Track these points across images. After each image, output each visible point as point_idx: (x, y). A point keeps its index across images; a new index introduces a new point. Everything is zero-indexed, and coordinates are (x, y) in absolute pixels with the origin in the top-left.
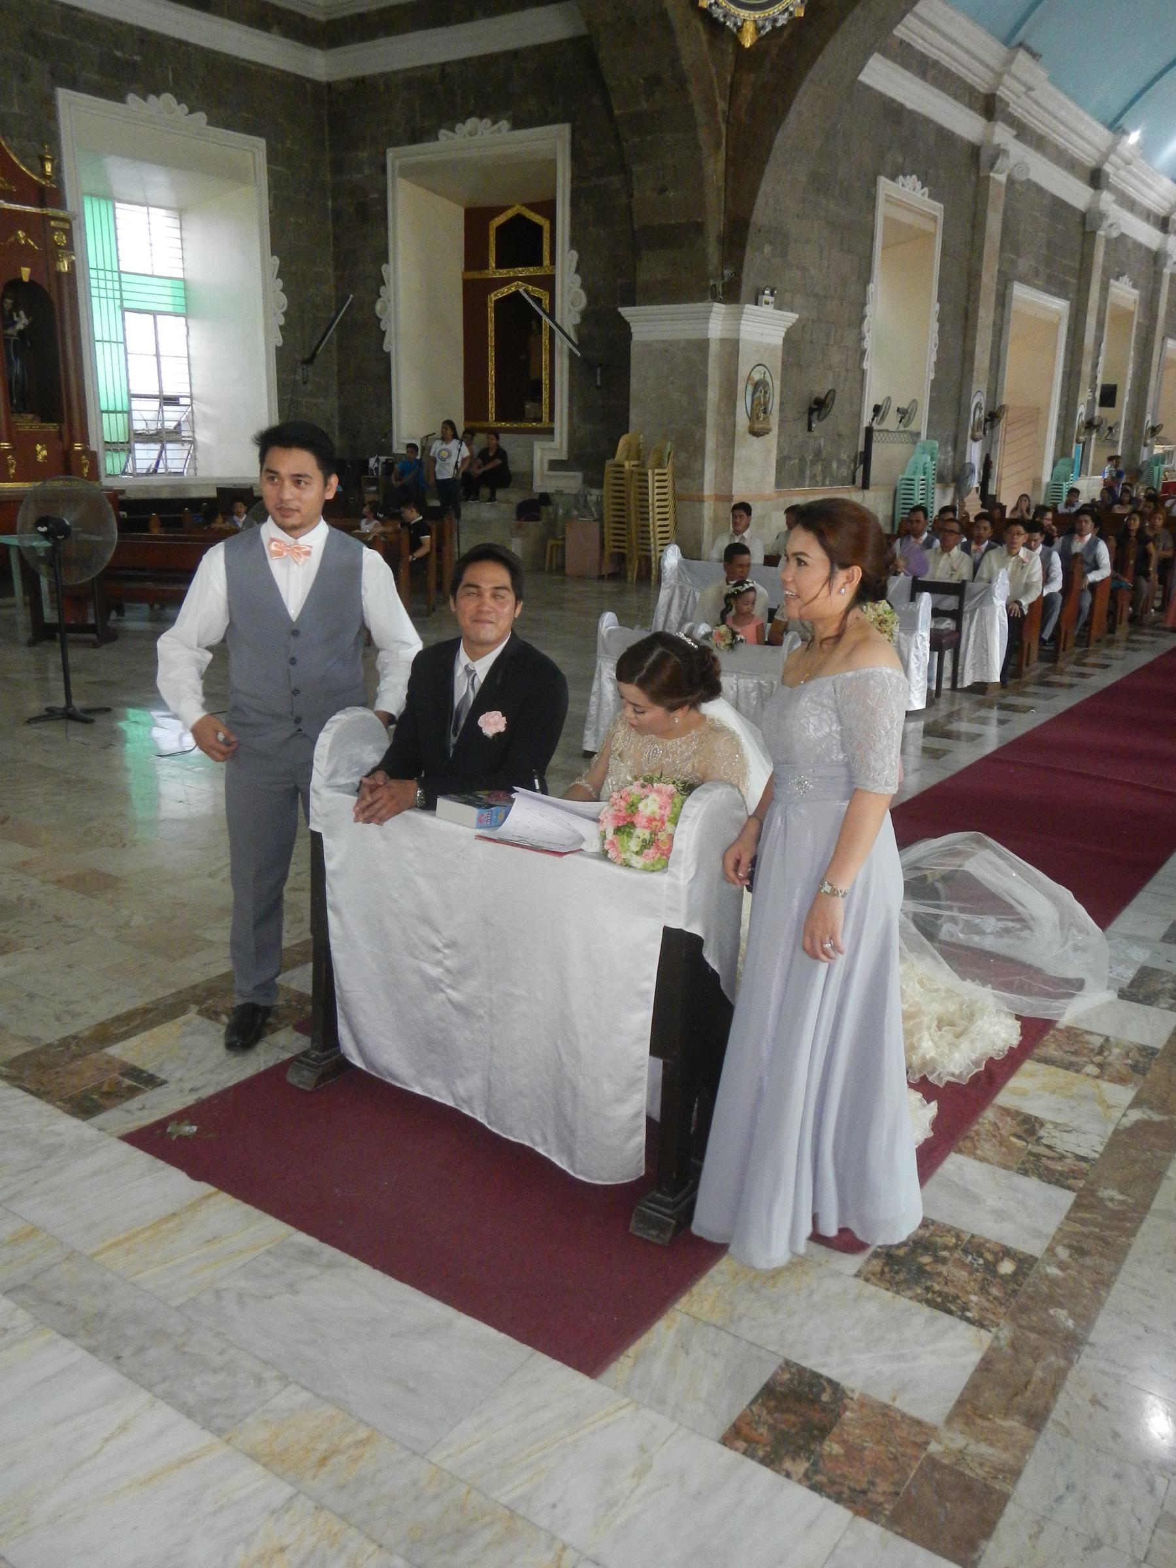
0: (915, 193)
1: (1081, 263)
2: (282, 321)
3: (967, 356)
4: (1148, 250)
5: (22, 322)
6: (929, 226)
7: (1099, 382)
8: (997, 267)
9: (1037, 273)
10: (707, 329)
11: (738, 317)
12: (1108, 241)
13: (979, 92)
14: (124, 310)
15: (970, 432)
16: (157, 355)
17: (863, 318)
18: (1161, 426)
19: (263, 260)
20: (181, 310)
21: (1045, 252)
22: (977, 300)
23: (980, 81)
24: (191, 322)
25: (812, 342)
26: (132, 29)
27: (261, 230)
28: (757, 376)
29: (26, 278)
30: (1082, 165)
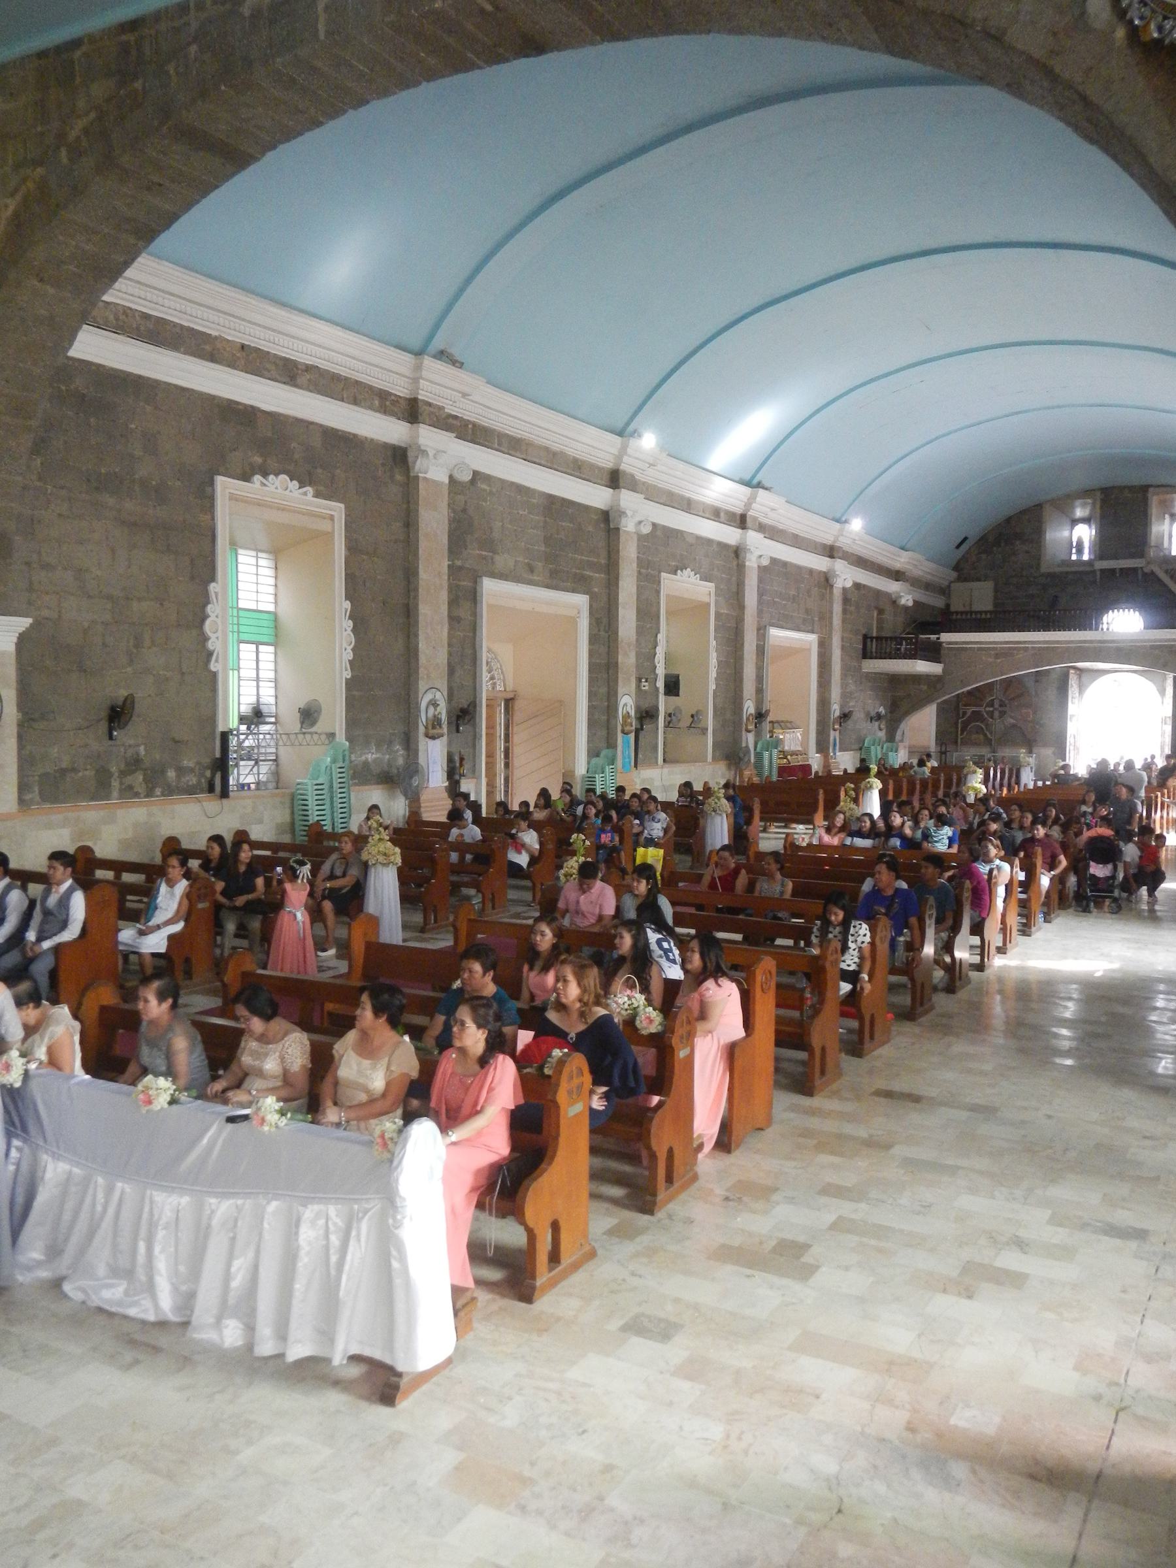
0: (287, 492)
1: (609, 557)
3: (411, 654)
4: (723, 546)
6: (325, 526)
7: (661, 671)
8: (446, 563)
12: (641, 538)
13: (396, 395)
15: (422, 729)
17: (204, 617)
18: (768, 712)
21: (543, 549)
22: (416, 597)
23: (401, 389)
25: (105, 645)
30: (593, 467)
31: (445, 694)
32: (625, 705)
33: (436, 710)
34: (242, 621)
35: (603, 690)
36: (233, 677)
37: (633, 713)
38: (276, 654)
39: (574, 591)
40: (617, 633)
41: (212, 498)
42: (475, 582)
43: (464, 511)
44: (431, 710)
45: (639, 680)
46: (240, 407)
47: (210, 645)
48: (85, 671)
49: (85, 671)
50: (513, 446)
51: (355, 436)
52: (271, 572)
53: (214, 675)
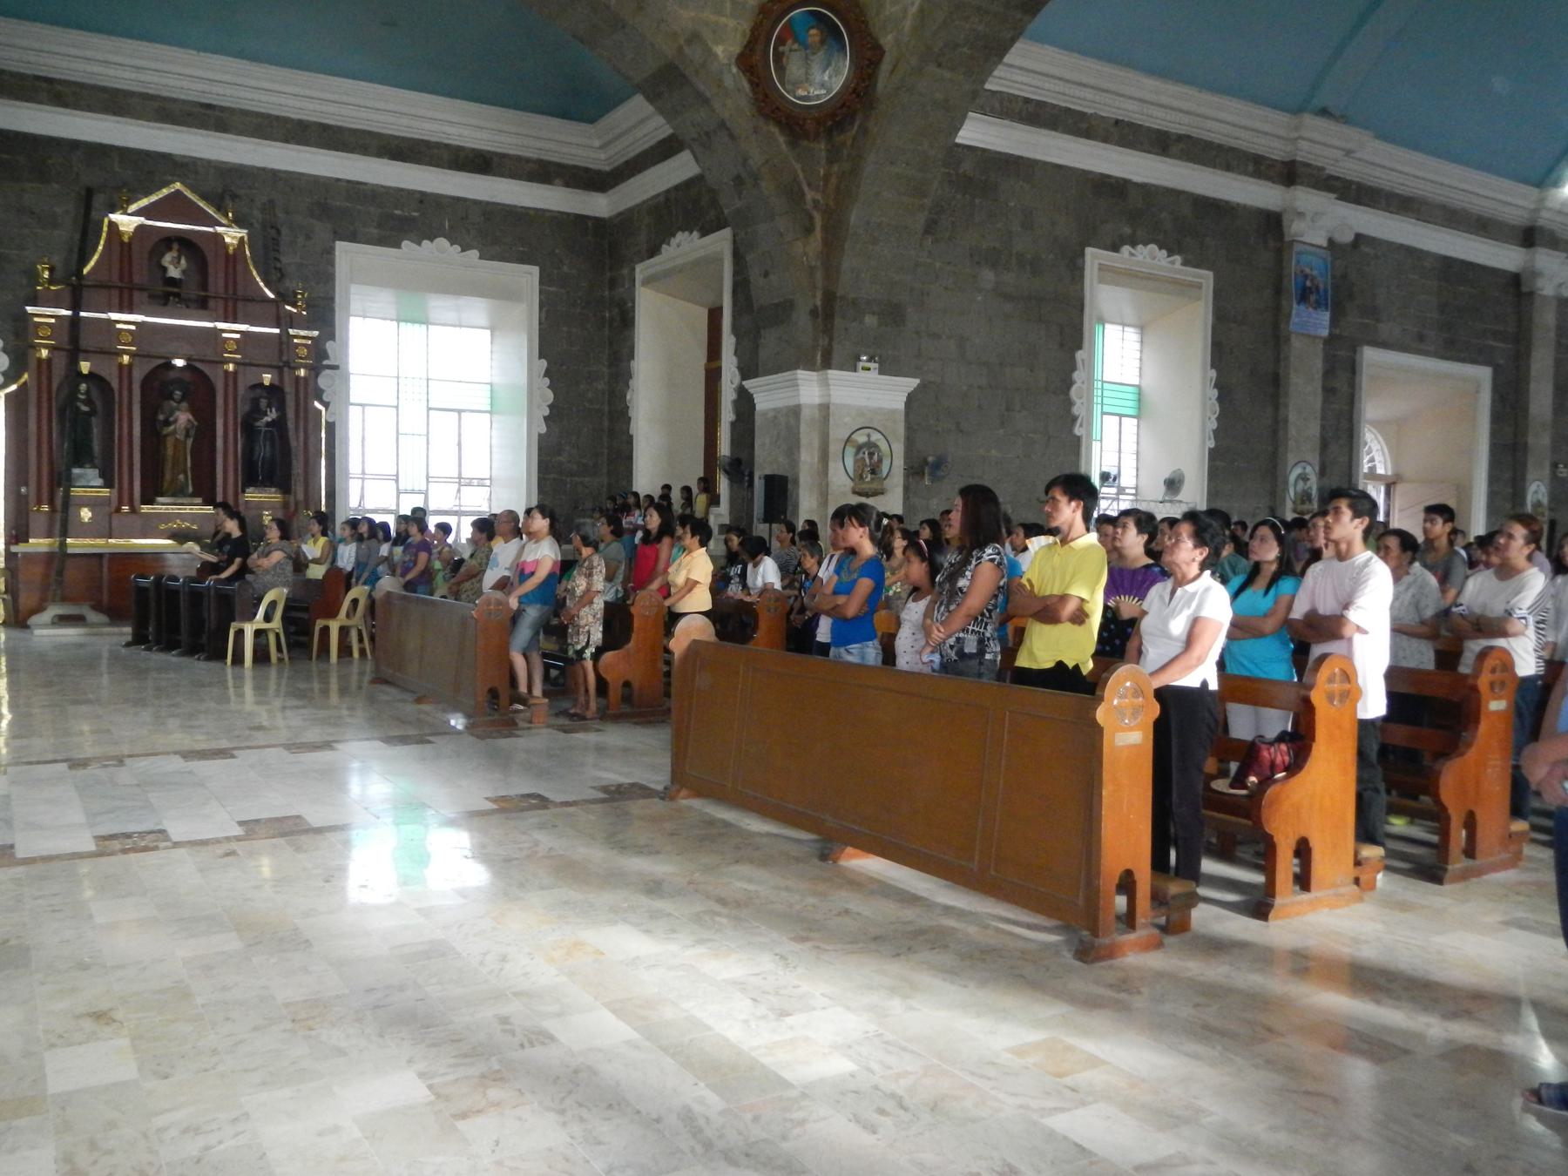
2: (547, 412)
5: (272, 415)
9: (1421, 338)
10: (798, 395)
11: (825, 384)
13: (1272, 160)
14: (429, 409)
16: (459, 444)
17: (1068, 383)
19: (530, 362)
20: (489, 408)
24: (495, 417)
26: (411, 193)
27: (530, 340)
28: (861, 438)
29: (267, 383)
31: (1317, 468)
32: (1536, 492)
33: (1305, 484)
34: (1105, 393)
35: (1507, 475)
36: (1096, 446)
37: (1545, 501)
38: (1138, 426)
39: (1474, 362)
40: (1526, 410)
41: (1082, 269)
42: (1355, 352)
43: (1344, 276)
44: (1301, 485)
45: (1555, 466)
46: (1113, 181)
47: (1075, 410)
48: (961, 431)
49: (961, 431)
50: (1404, 205)
51: (1227, 202)
52: (1137, 346)
53: (1079, 439)
